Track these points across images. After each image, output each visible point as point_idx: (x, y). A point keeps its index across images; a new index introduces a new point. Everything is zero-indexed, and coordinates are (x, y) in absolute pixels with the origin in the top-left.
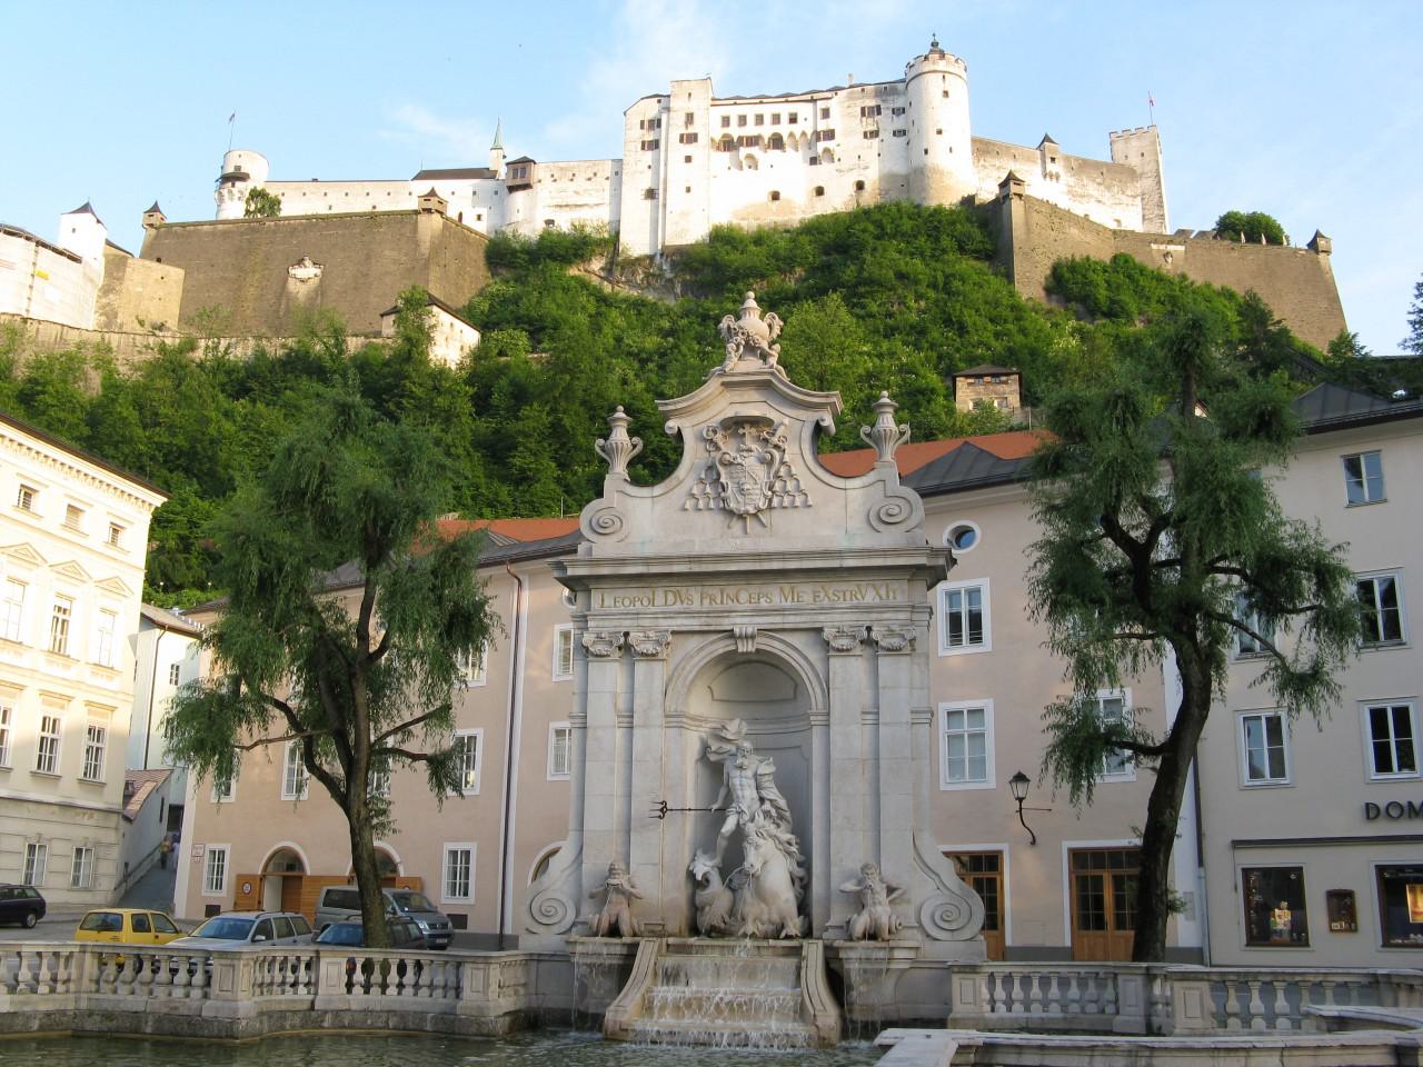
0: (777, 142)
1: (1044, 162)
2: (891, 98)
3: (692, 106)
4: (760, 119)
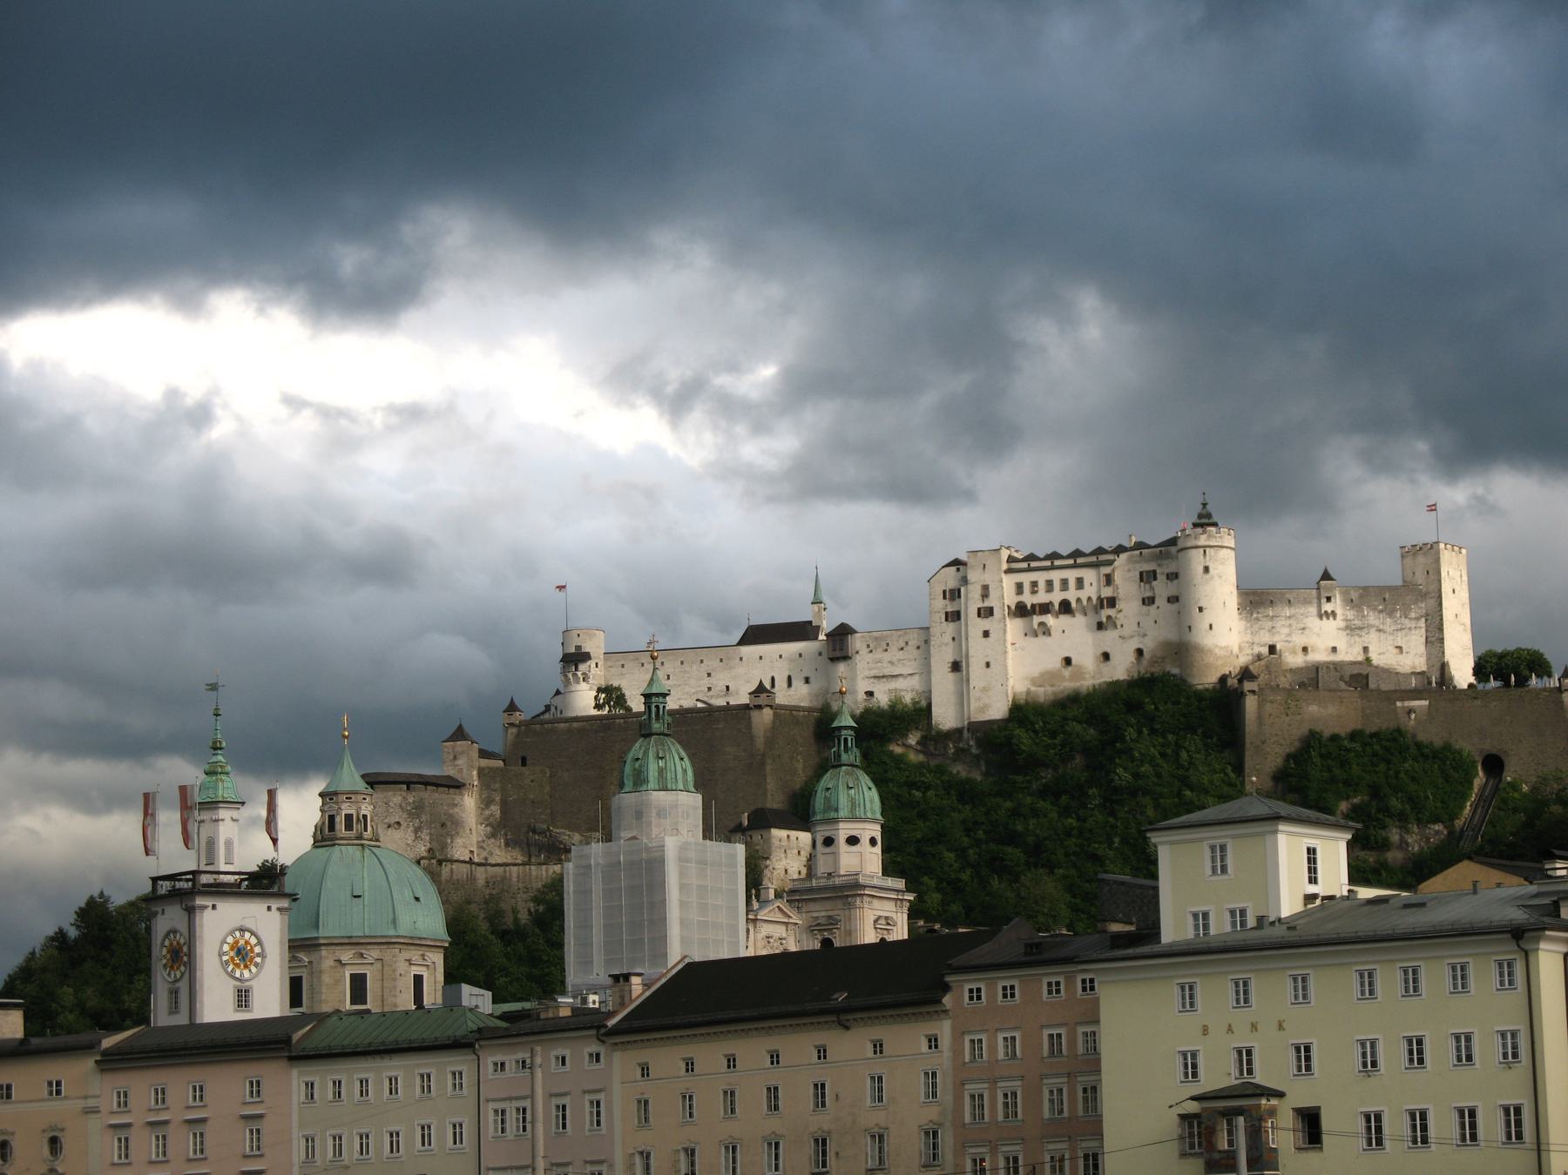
0: (1065, 607)
1: (1319, 599)
2: (1165, 562)
3: (987, 578)
4: (1050, 584)
